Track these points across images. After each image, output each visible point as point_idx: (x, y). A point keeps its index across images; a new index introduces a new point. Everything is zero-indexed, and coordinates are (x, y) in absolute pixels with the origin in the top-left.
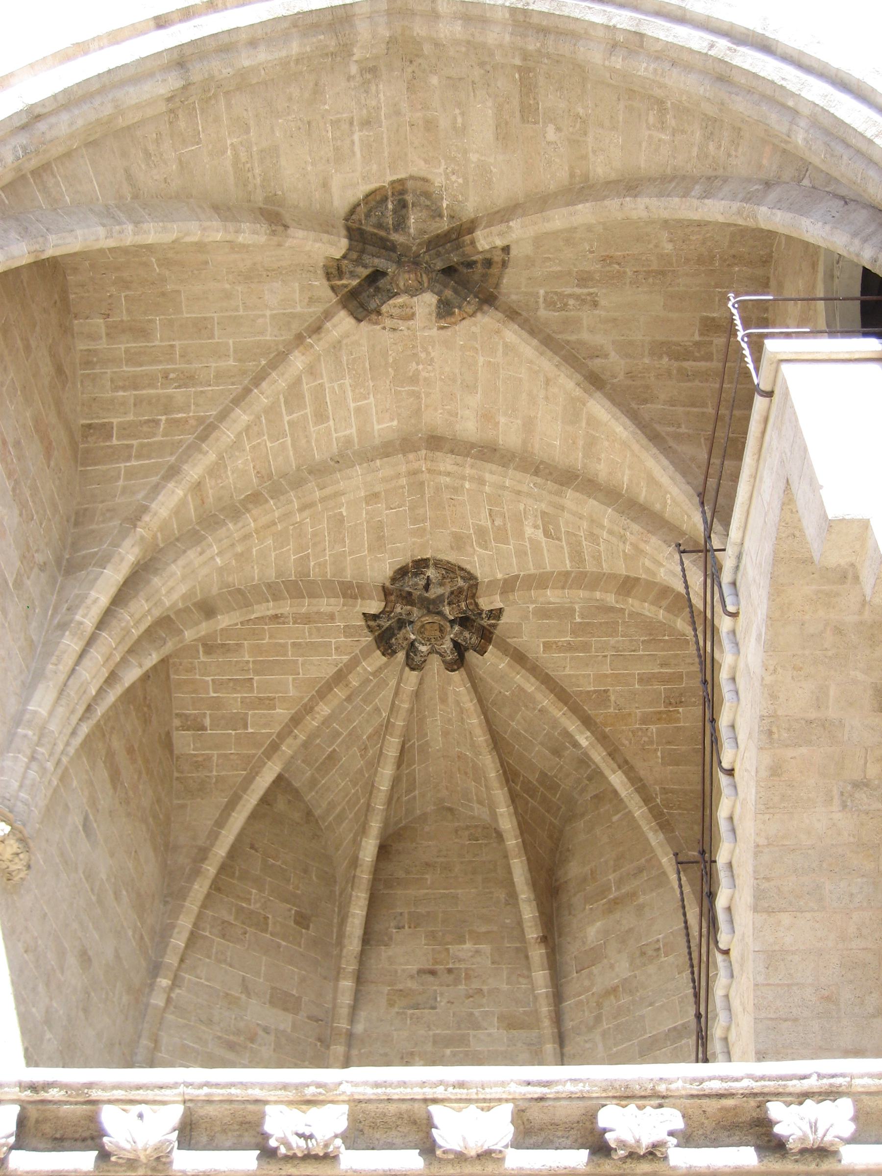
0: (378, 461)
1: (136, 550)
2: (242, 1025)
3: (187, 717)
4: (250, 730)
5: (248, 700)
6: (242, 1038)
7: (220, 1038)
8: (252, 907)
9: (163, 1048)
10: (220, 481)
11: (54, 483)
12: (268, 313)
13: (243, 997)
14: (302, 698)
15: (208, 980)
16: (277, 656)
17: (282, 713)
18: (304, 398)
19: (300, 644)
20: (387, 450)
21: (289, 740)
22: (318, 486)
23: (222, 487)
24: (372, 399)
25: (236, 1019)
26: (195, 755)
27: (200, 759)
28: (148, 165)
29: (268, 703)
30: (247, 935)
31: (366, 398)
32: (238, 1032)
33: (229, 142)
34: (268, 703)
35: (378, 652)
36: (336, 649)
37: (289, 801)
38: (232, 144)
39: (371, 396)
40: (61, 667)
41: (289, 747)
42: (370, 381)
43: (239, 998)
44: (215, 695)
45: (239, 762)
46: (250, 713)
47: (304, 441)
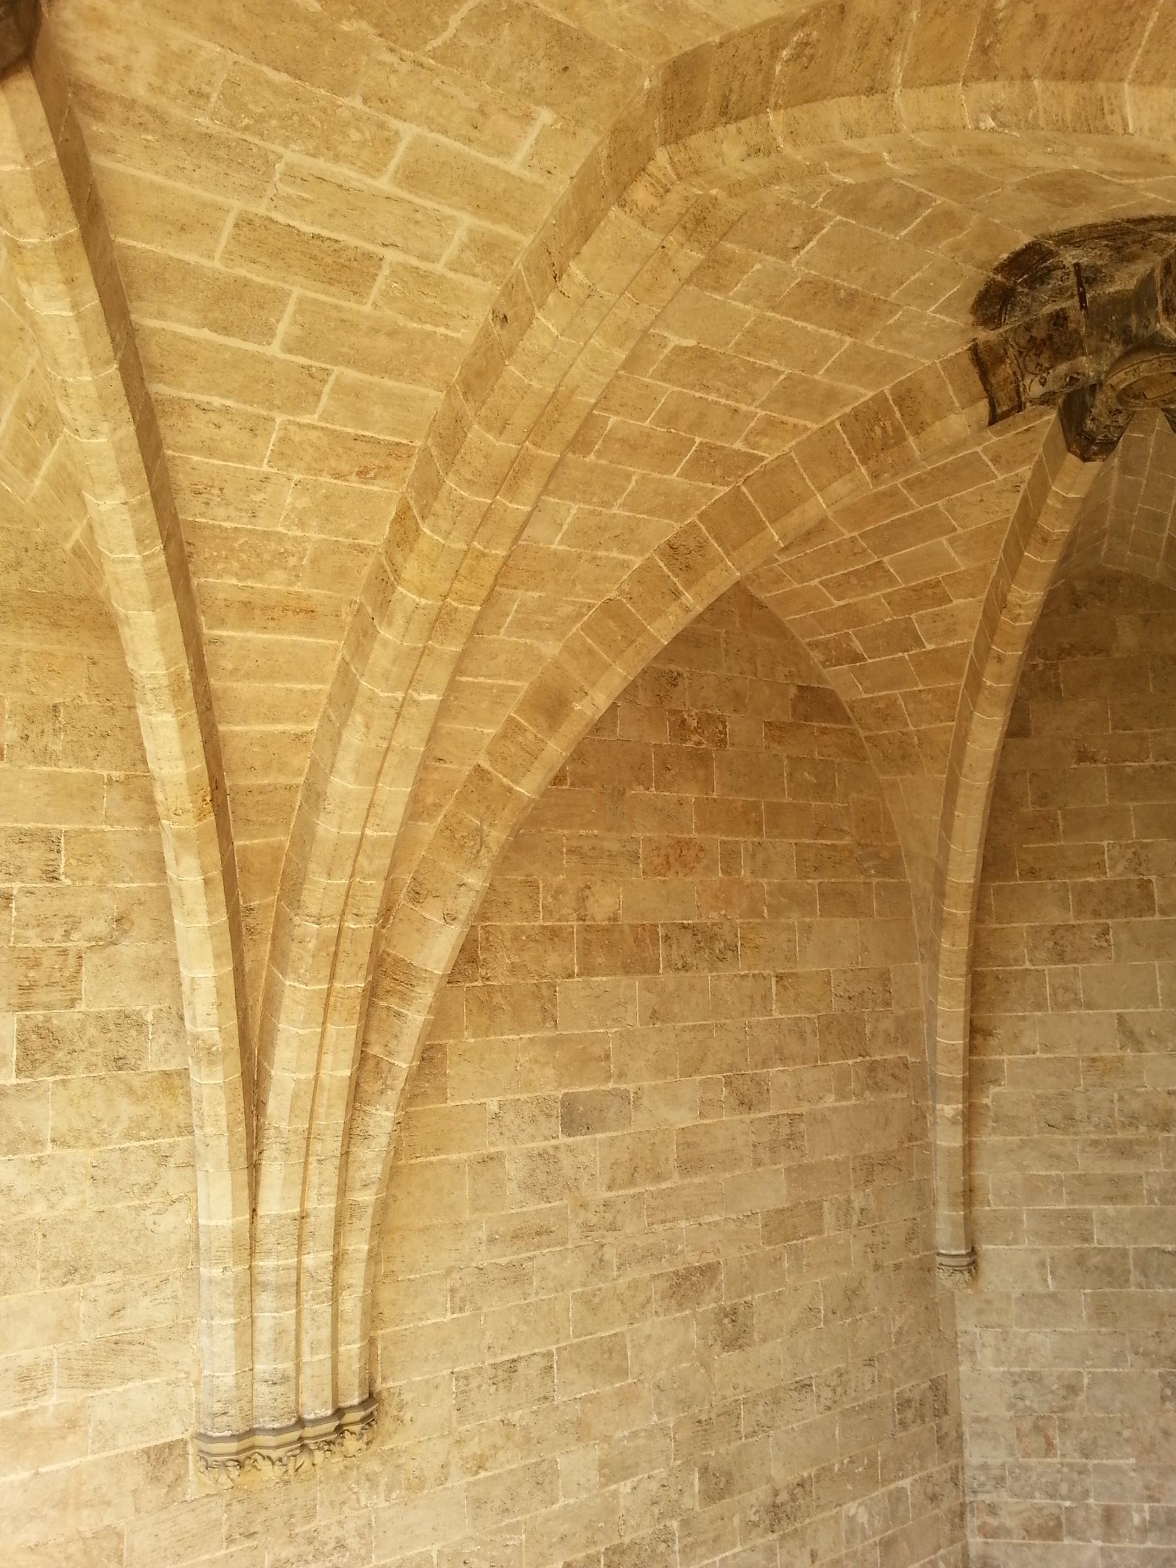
0: (574, 268)
1: (190, 862)
2: (1136, 1105)
3: (825, 644)
4: (930, 647)
5: (898, 598)
6: (1143, 1129)
7: (1096, 1143)
8: (1110, 876)
9: (990, 1197)
10: (292, 561)
11: (45, 756)
13: (1129, 1053)
14: (984, 569)
15: (1047, 1048)
16: (895, 512)
17: (966, 606)
18: (246, 283)
19: (919, 480)
20: (581, 224)
21: (992, 667)
22: (489, 429)
23: (314, 561)
24: (408, 131)
25: (1121, 1099)
26: (872, 700)
27: (881, 705)
29: (930, 594)
30: (1111, 936)
31: (390, 141)
32: (1133, 1120)
34: (930, 594)
35: (1072, 459)
36: (995, 460)
37: (1146, 620)
39: (395, 124)
40: (209, 1130)
41: (999, 678)
42: (340, 101)
43: (1121, 1059)
44: (842, 603)
45: (937, 705)
46: (913, 616)
47: (382, 342)
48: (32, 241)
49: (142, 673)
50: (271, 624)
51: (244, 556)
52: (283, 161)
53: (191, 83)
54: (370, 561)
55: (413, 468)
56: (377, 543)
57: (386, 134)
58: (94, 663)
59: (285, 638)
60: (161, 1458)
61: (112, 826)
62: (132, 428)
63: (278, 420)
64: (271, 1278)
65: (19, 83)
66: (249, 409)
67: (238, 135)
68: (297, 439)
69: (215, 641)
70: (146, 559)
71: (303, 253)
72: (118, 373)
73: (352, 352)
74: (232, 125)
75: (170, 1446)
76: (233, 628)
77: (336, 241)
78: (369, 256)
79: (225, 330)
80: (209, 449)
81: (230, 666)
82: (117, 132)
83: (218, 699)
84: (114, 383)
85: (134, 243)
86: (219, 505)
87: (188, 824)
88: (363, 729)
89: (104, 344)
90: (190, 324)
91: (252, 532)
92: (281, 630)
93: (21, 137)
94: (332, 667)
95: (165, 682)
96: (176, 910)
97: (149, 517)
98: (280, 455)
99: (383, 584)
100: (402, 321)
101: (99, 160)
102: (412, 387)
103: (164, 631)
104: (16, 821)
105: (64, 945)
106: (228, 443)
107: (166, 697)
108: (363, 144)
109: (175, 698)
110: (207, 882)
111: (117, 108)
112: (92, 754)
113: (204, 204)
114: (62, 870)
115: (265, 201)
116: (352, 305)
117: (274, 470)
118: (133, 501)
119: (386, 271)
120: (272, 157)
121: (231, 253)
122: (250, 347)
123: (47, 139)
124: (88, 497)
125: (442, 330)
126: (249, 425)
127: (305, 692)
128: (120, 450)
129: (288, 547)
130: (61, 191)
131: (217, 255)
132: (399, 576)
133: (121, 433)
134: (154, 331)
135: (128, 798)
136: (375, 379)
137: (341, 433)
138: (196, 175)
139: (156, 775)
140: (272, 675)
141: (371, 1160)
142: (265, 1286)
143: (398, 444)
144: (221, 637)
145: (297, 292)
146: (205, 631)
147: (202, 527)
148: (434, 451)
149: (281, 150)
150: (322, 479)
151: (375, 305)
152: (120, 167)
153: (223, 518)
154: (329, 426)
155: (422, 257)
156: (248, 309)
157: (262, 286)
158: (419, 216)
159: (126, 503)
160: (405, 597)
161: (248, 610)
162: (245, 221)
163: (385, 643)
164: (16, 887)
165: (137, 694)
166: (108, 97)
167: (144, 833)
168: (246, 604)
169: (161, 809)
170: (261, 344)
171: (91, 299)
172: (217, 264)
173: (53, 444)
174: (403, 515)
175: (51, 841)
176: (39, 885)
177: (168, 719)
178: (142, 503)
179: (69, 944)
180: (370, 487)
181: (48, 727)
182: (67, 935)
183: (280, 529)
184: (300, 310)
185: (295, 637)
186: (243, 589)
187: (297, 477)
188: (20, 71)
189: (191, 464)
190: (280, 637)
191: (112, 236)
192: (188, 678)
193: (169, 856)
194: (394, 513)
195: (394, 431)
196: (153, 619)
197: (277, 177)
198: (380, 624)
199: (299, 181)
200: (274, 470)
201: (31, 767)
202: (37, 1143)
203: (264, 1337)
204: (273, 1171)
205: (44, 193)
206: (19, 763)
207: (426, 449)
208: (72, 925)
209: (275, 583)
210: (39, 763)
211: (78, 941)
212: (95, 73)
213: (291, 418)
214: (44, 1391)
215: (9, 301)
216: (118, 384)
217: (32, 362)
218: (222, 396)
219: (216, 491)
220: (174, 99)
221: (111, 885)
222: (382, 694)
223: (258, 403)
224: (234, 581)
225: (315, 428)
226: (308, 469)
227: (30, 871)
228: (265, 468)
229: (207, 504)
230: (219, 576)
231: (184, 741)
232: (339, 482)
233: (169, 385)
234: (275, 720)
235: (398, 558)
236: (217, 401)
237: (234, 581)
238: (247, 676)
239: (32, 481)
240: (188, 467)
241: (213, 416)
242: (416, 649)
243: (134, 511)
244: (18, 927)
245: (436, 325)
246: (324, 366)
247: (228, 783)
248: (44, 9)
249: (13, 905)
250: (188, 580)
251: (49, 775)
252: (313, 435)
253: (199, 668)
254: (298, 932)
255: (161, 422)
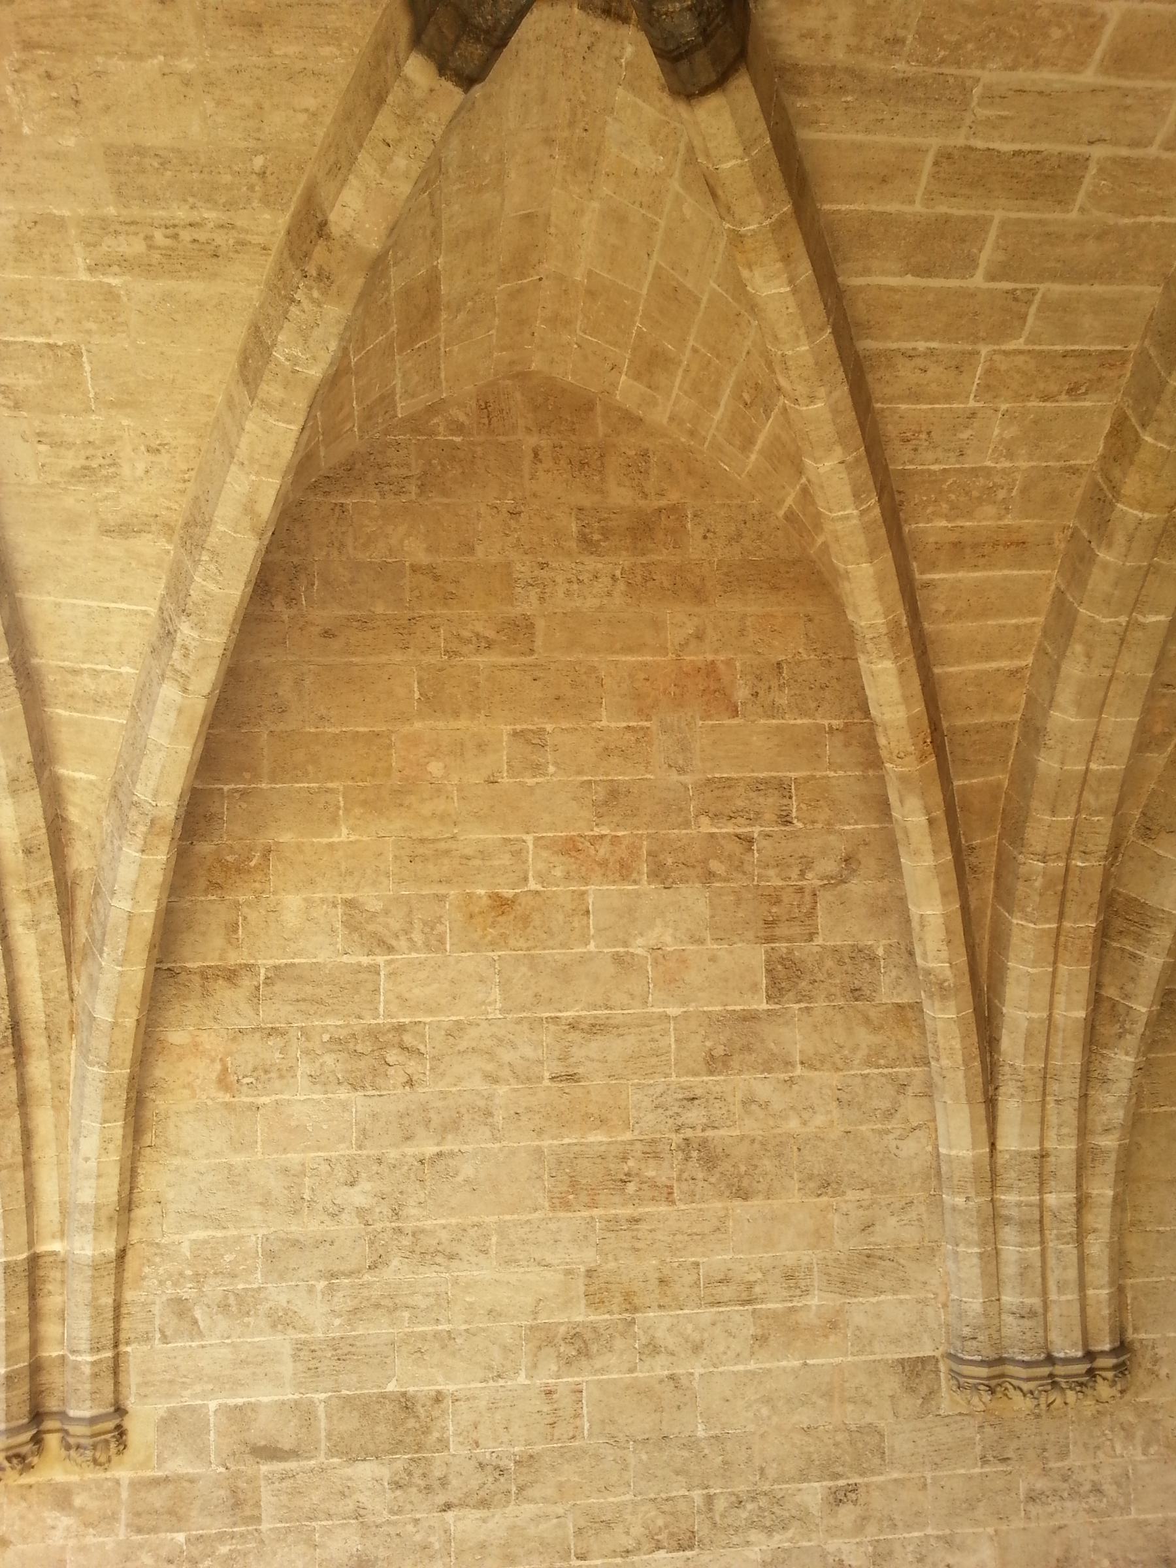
10: (1001, 494)
11: (773, 710)
12: (675, 185)
18: (947, 219)
23: (1024, 490)
28: (107, 480)
33: (84, 277)
38: (90, 270)
40: (945, 1062)
48: (751, 227)
49: (863, 624)
50: (982, 561)
51: (953, 497)
52: (981, 84)
53: (888, 33)
54: (1084, 481)
55: (1128, 375)
56: (1091, 461)
57: (1091, 20)
58: (810, 620)
59: (997, 573)
60: (915, 1370)
61: (835, 771)
62: (846, 388)
63: (984, 352)
64: (1014, 1212)
65: (736, 82)
66: (954, 346)
67: (935, 70)
68: (1003, 367)
69: (927, 585)
70: (862, 513)
71: (1003, 173)
72: (832, 337)
73: (1059, 265)
74: (928, 62)
75: (923, 1361)
76: (945, 570)
77: (1038, 152)
78: (1074, 159)
79: (928, 272)
80: (915, 396)
81: (942, 609)
82: (819, 103)
83: (932, 643)
84: (828, 347)
85: (839, 207)
86: (927, 449)
87: (911, 766)
88: (1084, 659)
89: (818, 313)
90: (894, 274)
91: (960, 471)
92: (991, 566)
93: (740, 132)
94: (1046, 599)
95: (884, 630)
96: (902, 850)
97: (864, 472)
98: (988, 389)
99: (1100, 506)
100: (1111, 219)
101: (805, 134)
102: (1125, 287)
103: (881, 580)
104: (753, 771)
105: (800, 883)
106: (934, 385)
107: (885, 644)
108: (1066, 39)
109: (893, 644)
110: (931, 822)
111: (818, 79)
112: (813, 705)
113: (904, 150)
114: (794, 814)
115: (964, 130)
116: (1058, 215)
117: (981, 404)
118: (849, 459)
119: (1093, 170)
120: (969, 83)
121: (931, 193)
122: (953, 283)
123: (762, 126)
124: (808, 461)
125: (1158, 218)
126: (954, 363)
127: (1017, 627)
128: (835, 411)
129: (997, 480)
130: (775, 174)
131: (918, 199)
132: (1118, 493)
133: (837, 394)
134: (861, 289)
135: (847, 745)
136: (1084, 288)
137: (1049, 352)
138: (894, 123)
139: (878, 720)
140: (984, 612)
141: (1112, 1104)
142: (1008, 1220)
143: (1111, 352)
144: (933, 580)
145: (998, 215)
146: (917, 576)
147: (913, 473)
148: (1153, 352)
149: (977, 72)
150: (1030, 404)
151: (1082, 209)
152: (822, 136)
153: (932, 462)
154: (1037, 348)
155: (1134, 144)
156: (949, 246)
157: (963, 219)
158: (1129, 101)
159: (842, 462)
160: (1125, 513)
161: (959, 551)
162: (945, 156)
163: (1105, 566)
164: (756, 830)
165: (858, 644)
166: (809, 71)
167: (865, 778)
168: (957, 545)
169: (884, 753)
170: (963, 278)
171: (805, 271)
172: (918, 207)
173: (768, 419)
174: (1120, 426)
175: (782, 788)
176: (776, 829)
177: (888, 664)
178: (857, 460)
179: (805, 883)
180: (1082, 404)
181: (774, 683)
182: (802, 874)
183: (989, 463)
184: (1003, 233)
185: (1006, 572)
186: (952, 529)
187: (1004, 407)
188: (737, 70)
189: (900, 412)
190: (990, 573)
191: (818, 205)
192: (905, 624)
193: (893, 798)
194: (1108, 427)
195: (1105, 340)
196: (871, 571)
197: (974, 104)
198: (1099, 546)
199: (998, 100)
200: (981, 404)
201: (762, 721)
202: (788, 1064)
203: (1010, 1270)
204: (1010, 1108)
205: (760, 177)
206: (752, 718)
207: (1143, 352)
208: (807, 863)
209: (985, 519)
210: (768, 717)
211: (812, 880)
212: (798, 51)
213: (996, 347)
214: (806, 1292)
215: (727, 291)
216: (832, 348)
217: (748, 343)
218: (927, 340)
219: (923, 436)
220: (871, 53)
221: (838, 827)
222: (1105, 621)
223: (962, 339)
224: (944, 523)
225: (1021, 352)
226: (1017, 397)
227: (767, 816)
228: (972, 404)
229: (915, 450)
230: (929, 520)
231: (903, 686)
232: (1048, 404)
233: (875, 339)
234: (989, 658)
235: (1116, 473)
236: (922, 346)
237: (944, 523)
238: (960, 616)
239: (748, 457)
240: (896, 417)
241: (919, 362)
242: (1140, 568)
243: (850, 468)
244: (760, 867)
245: (1151, 215)
246: (1029, 286)
247: (945, 724)
248: (751, 5)
249: (755, 847)
250: (900, 529)
251: (777, 727)
252: (1020, 360)
253: (914, 614)
254: (1023, 870)
255: (870, 378)
